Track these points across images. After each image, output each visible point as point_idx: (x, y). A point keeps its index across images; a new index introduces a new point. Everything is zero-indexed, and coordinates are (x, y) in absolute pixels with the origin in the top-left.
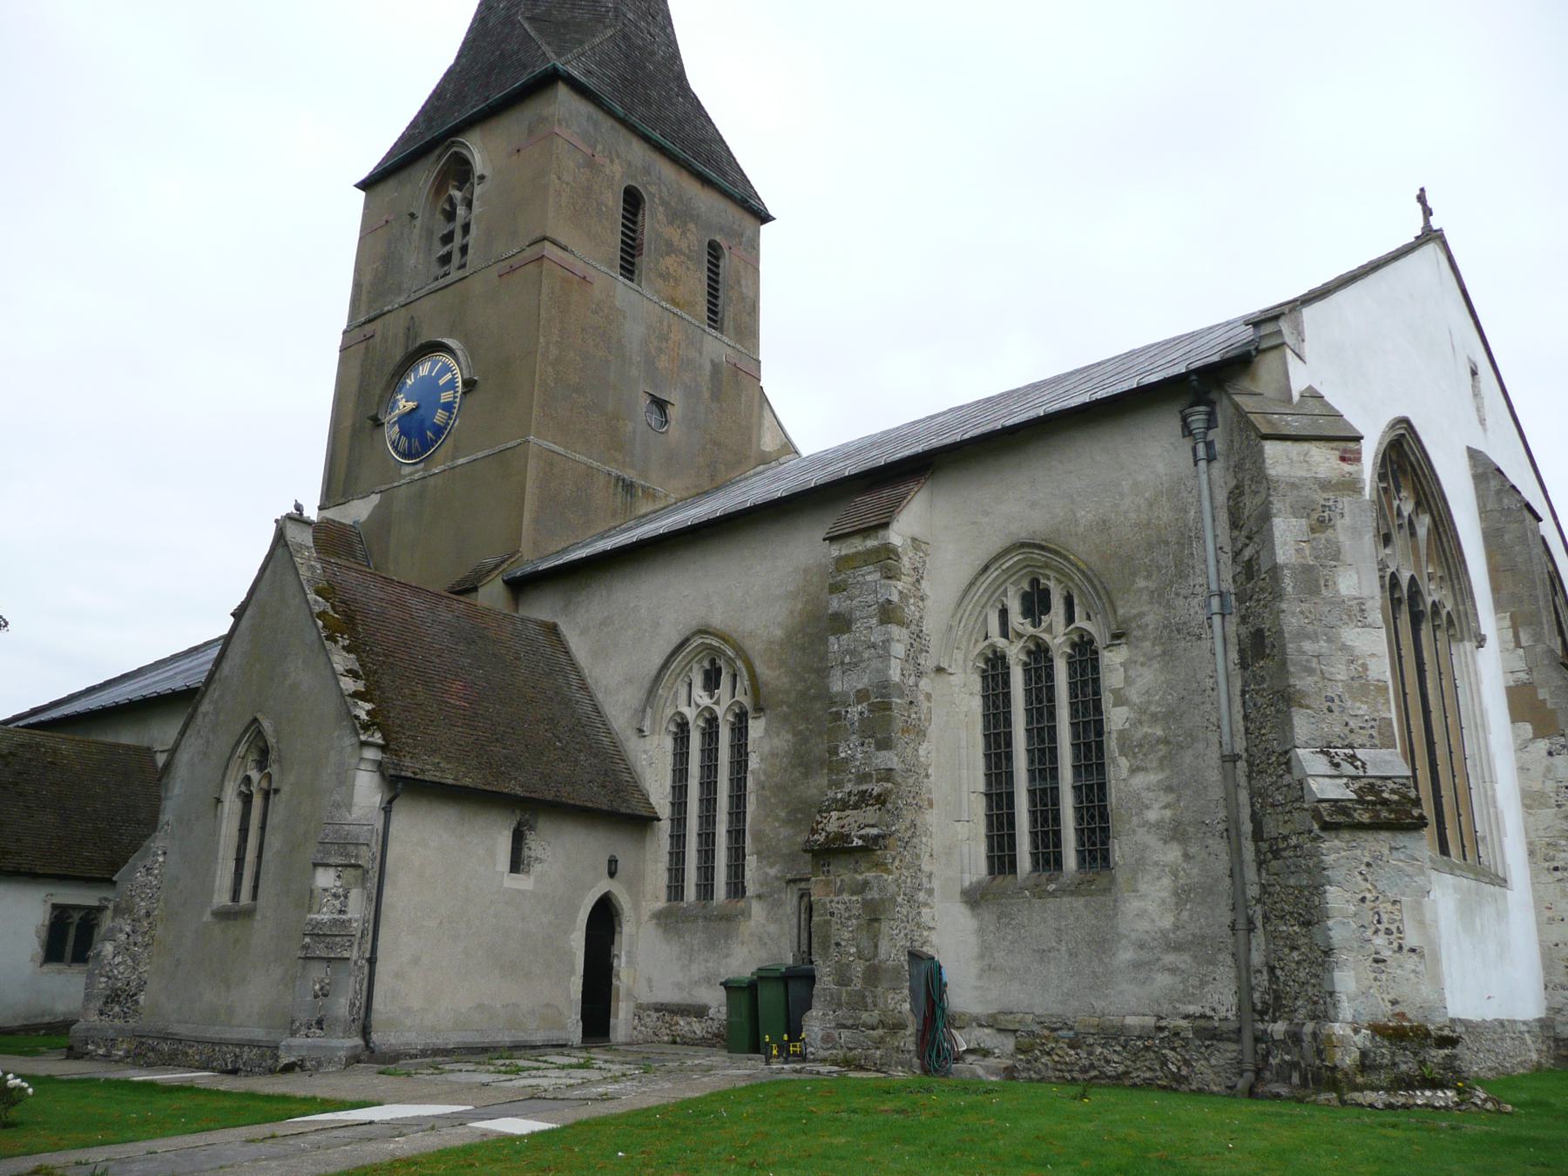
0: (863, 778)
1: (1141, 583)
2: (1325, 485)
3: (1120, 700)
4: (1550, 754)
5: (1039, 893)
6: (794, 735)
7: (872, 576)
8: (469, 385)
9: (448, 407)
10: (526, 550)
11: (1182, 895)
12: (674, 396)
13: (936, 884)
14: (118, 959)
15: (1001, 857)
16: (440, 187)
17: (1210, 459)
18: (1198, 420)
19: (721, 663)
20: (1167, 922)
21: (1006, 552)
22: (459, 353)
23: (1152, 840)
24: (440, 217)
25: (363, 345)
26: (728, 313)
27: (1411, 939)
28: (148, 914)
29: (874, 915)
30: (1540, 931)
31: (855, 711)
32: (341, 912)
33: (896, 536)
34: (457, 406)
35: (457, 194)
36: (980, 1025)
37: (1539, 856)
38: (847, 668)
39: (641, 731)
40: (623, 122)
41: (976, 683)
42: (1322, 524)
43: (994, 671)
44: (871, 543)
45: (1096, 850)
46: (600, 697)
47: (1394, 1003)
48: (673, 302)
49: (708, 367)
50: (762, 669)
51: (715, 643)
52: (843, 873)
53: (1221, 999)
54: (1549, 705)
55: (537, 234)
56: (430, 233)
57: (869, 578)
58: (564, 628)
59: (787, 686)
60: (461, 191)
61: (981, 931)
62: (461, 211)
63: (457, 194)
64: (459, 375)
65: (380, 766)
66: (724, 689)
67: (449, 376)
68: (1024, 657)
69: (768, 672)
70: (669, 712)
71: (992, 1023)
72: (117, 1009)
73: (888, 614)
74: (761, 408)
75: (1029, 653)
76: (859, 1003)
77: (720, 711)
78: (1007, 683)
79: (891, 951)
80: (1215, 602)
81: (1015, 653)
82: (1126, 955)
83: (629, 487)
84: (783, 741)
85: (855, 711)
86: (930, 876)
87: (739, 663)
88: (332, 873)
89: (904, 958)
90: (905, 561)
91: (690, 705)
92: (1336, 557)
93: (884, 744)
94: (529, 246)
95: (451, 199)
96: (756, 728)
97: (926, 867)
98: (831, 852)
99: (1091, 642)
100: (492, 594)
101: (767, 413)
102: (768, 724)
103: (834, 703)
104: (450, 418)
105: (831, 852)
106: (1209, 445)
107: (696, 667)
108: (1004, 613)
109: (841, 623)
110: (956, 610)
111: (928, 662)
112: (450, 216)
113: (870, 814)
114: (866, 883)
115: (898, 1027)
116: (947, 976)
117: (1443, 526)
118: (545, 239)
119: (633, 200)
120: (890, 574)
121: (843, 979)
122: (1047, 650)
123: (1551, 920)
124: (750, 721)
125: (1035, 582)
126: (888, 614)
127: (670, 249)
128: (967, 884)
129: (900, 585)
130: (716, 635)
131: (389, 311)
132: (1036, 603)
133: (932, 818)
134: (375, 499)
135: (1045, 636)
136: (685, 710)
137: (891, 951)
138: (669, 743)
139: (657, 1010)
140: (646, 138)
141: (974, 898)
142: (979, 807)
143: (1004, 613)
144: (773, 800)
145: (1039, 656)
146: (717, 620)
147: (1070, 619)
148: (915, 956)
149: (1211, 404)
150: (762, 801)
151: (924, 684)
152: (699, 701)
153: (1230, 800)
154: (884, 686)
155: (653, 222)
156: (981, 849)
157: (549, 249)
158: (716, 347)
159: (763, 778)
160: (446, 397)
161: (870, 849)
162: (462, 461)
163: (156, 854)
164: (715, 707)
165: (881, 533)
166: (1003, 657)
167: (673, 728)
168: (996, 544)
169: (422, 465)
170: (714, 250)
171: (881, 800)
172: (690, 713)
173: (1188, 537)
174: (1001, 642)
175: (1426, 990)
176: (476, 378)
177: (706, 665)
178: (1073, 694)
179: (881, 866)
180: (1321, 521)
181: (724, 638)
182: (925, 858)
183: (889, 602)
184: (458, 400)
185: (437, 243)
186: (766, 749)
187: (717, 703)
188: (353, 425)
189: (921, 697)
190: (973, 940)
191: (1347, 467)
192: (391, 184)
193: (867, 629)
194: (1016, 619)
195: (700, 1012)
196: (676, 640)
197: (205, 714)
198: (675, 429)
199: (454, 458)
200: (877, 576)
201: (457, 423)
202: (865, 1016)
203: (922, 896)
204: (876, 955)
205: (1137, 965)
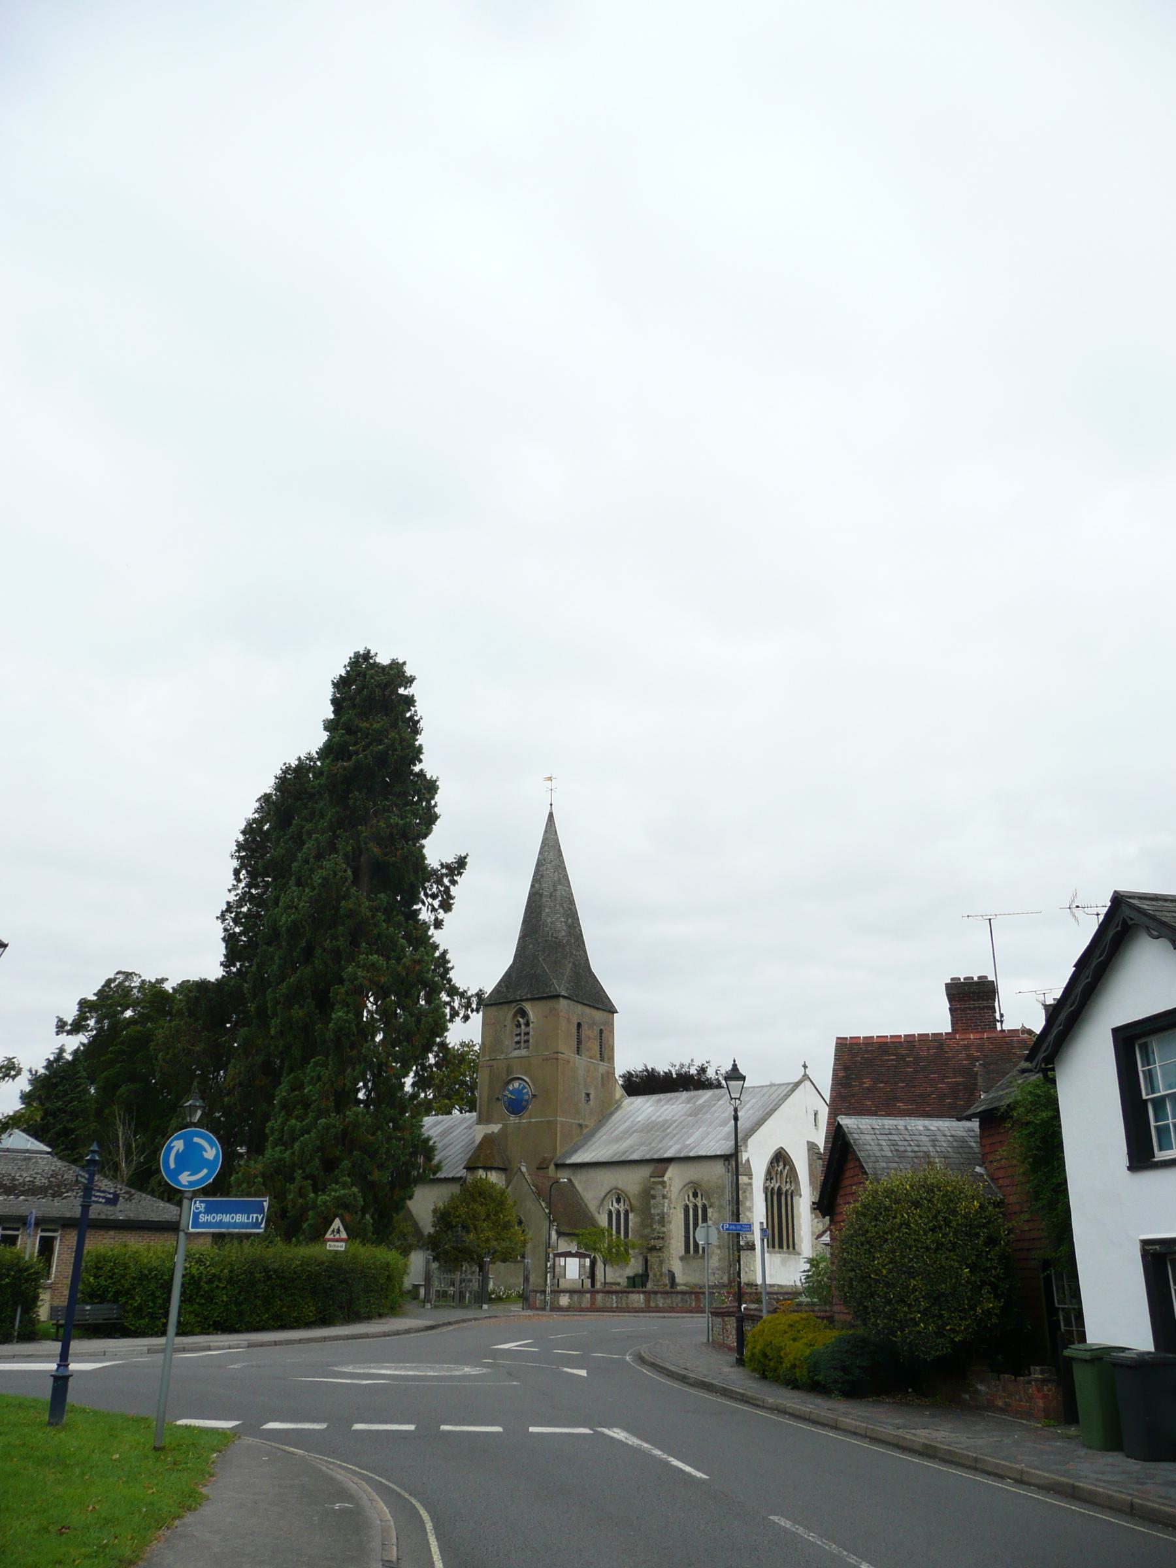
0: (659, 1233)
1: (715, 1195)
2: (745, 1184)
3: (711, 1220)
5: (694, 1258)
7: (660, 1187)
10: (558, 1154)
11: (720, 1260)
15: (687, 1250)
16: (515, 1016)
20: (717, 1265)
21: (689, 1183)
23: (715, 1248)
24: (515, 1027)
27: (752, 1268)
29: (661, 1262)
31: (657, 1218)
33: (666, 1179)
35: (521, 1020)
38: (655, 1208)
39: (599, 1213)
40: (578, 1002)
41: (683, 1211)
43: (686, 1208)
44: (660, 1179)
46: (586, 1201)
48: (591, 1058)
49: (600, 1076)
52: (654, 1254)
53: (725, 1280)
56: (512, 1032)
61: (683, 1266)
62: (523, 1027)
63: (521, 1020)
65: (556, 1231)
66: (622, 1204)
71: (685, 1285)
73: (664, 1197)
76: (658, 1281)
77: (621, 1209)
79: (665, 1270)
81: (691, 1206)
83: (581, 1126)
84: (638, 1219)
85: (657, 1218)
87: (626, 1199)
93: (663, 1226)
95: (518, 1021)
96: (631, 1216)
98: (652, 1249)
100: (552, 1167)
105: (652, 1249)
108: (689, 1196)
109: (654, 1197)
111: (672, 1206)
112: (519, 1026)
113: (660, 1241)
115: (666, 1286)
116: (676, 1275)
117: (793, 1169)
118: (558, 1053)
119: (579, 1025)
120: (665, 1187)
121: (655, 1276)
126: (664, 1197)
127: (589, 1038)
132: (695, 1195)
133: (672, 1241)
134: (500, 1126)
136: (611, 1207)
137: (665, 1270)
138: (606, 1216)
140: (581, 1003)
141: (682, 1259)
142: (683, 1239)
143: (689, 1196)
145: (696, 1207)
146: (620, 1186)
148: (669, 1271)
153: (729, 1242)
155: (586, 1032)
158: (603, 1067)
160: (526, 1097)
161: (661, 1249)
162: (533, 1120)
171: (663, 1238)
172: (613, 1209)
175: (754, 1277)
179: (663, 1252)
181: (622, 1192)
190: (681, 1268)
192: (494, 1008)
193: (659, 1199)
195: (619, 1284)
196: (608, 1190)
198: (592, 1102)
199: (530, 1118)
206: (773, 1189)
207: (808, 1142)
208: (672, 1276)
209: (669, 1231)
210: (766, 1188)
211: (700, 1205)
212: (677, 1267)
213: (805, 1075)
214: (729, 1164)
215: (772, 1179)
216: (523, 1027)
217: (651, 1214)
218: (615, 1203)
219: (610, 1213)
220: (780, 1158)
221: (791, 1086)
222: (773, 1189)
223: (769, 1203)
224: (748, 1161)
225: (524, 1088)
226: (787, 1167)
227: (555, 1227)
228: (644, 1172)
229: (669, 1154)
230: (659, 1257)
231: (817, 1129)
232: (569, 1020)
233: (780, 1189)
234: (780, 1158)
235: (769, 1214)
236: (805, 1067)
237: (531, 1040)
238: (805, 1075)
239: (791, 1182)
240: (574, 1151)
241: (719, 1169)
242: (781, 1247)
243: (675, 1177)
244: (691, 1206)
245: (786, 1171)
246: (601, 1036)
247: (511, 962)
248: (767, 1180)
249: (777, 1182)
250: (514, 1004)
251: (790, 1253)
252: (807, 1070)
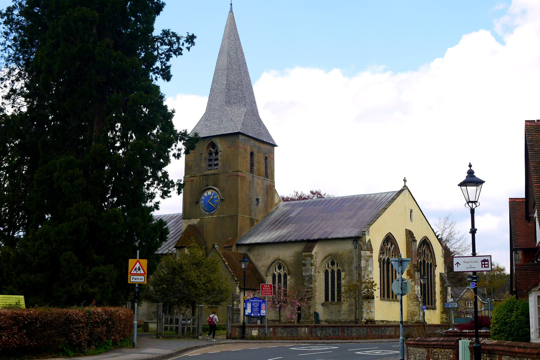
0: (308, 288)
2: (368, 256)
4: (411, 281)
5: (332, 304)
8: (222, 200)
12: (260, 197)
13: (318, 303)
15: (327, 299)
16: (208, 147)
17: (356, 248)
18: (355, 243)
19: (282, 265)
22: (219, 192)
25: (190, 182)
26: (270, 176)
27: (372, 311)
30: (407, 308)
33: (313, 253)
35: (212, 150)
36: (324, 321)
37: (408, 297)
39: (267, 275)
41: (324, 274)
42: (367, 261)
43: (326, 273)
44: (309, 254)
45: (339, 300)
47: (369, 317)
49: (266, 188)
50: (290, 268)
51: (281, 262)
54: (412, 274)
55: (236, 170)
57: (309, 259)
58: (248, 254)
60: (214, 149)
62: (214, 155)
64: (219, 196)
66: (282, 270)
67: (216, 196)
68: (331, 271)
70: (272, 272)
71: (326, 321)
73: (312, 265)
74: (275, 193)
75: (332, 271)
77: (282, 273)
78: (328, 274)
79: (312, 312)
80: (355, 268)
81: (330, 270)
82: (343, 312)
86: (317, 301)
88: (236, 302)
89: (313, 313)
90: (314, 256)
91: (275, 271)
92: (369, 266)
93: (311, 284)
94: (234, 172)
95: (210, 151)
97: (316, 300)
99: (340, 270)
100: (234, 247)
101: (276, 194)
102: (291, 276)
103: (303, 277)
106: (356, 247)
107: (277, 265)
108: (328, 264)
109: (305, 265)
110: (321, 263)
111: (317, 271)
114: (309, 303)
119: (252, 154)
120: (312, 259)
122: (334, 270)
123: (409, 307)
124: (288, 276)
125: (333, 260)
126: (312, 265)
128: (322, 303)
129: (313, 260)
130: (281, 261)
131: (197, 176)
132: (333, 263)
133: (317, 293)
134: (199, 220)
135: (334, 269)
138: (272, 277)
139: (272, 321)
141: (323, 305)
142: (324, 292)
143: (328, 264)
145: (333, 271)
146: (281, 258)
147: (337, 267)
148: (315, 313)
149: (357, 241)
151: (316, 274)
152: (277, 271)
154: (311, 275)
155: (255, 159)
156: (324, 298)
157: (240, 173)
158: (267, 182)
162: (221, 216)
164: (281, 273)
165: (311, 252)
166: (328, 271)
167: (272, 275)
168: (326, 254)
170: (266, 158)
172: (276, 273)
173: (353, 258)
174: (328, 269)
176: (223, 198)
177: (279, 265)
178: (337, 277)
180: (367, 261)
182: (316, 299)
183: (312, 263)
184: (219, 202)
185: (208, 161)
187: (281, 272)
189: (316, 276)
191: (371, 254)
194: (330, 265)
198: (260, 204)
200: (310, 259)
201: (219, 207)
202: (309, 320)
203: (316, 304)
204: (310, 312)
205: (344, 314)
206: (384, 260)
207: (406, 229)
208: (316, 315)
209: (315, 287)
210: (380, 260)
211: (336, 270)
212: (320, 309)
213: (405, 186)
214: (357, 244)
215: (383, 253)
216: (214, 155)
217: (303, 276)
218: (277, 270)
219: (274, 276)
220: (389, 239)
221: (395, 194)
222: (384, 260)
223: (382, 269)
224: (369, 241)
225: (215, 195)
226: (393, 246)
227: (238, 285)
228: (298, 248)
229: (316, 237)
230: (308, 303)
231: (412, 221)
232: (245, 149)
233: (388, 259)
234: (389, 239)
235: (382, 275)
236: (405, 180)
237: (219, 164)
238: (405, 186)
239: (395, 256)
240: (249, 236)
241: (349, 246)
242: (388, 297)
243: (318, 252)
244: (330, 270)
245: (392, 248)
246: (266, 161)
247: (204, 112)
248: (381, 254)
249: (387, 256)
250: (207, 140)
251: (394, 301)
252: (406, 183)
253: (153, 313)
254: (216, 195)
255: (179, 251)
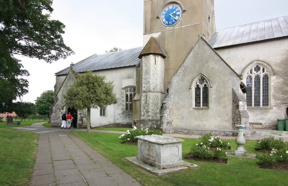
6: (284, 79)
9: (179, 15)
14: (168, 117)
28: (172, 109)
32: (244, 109)
34: (181, 15)
50: (274, 67)
59: (282, 71)
67: (178, 9)
69: (277, 68)
72: (169, 125)
104: (179, 18)
134: (160, 33)
144: (278, 90)
146: (261, 58)
150: (275, 90)
152: (254, 73)
159: (275, 86)
162: (183, 27)
163: (172, 98)
169: (172, 27)
184: (181, 14)
186: (276, 81)
187: (260, 73)
188: (151, 18)
196: (249, 62)
197: (180, 73)
253: (119, 115)
254: (178, 8)
255: (144, 59)
